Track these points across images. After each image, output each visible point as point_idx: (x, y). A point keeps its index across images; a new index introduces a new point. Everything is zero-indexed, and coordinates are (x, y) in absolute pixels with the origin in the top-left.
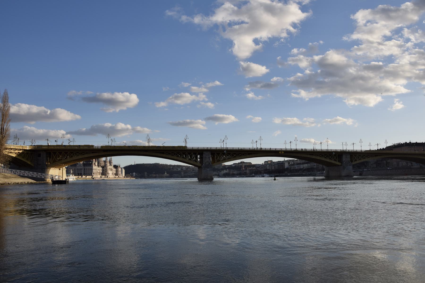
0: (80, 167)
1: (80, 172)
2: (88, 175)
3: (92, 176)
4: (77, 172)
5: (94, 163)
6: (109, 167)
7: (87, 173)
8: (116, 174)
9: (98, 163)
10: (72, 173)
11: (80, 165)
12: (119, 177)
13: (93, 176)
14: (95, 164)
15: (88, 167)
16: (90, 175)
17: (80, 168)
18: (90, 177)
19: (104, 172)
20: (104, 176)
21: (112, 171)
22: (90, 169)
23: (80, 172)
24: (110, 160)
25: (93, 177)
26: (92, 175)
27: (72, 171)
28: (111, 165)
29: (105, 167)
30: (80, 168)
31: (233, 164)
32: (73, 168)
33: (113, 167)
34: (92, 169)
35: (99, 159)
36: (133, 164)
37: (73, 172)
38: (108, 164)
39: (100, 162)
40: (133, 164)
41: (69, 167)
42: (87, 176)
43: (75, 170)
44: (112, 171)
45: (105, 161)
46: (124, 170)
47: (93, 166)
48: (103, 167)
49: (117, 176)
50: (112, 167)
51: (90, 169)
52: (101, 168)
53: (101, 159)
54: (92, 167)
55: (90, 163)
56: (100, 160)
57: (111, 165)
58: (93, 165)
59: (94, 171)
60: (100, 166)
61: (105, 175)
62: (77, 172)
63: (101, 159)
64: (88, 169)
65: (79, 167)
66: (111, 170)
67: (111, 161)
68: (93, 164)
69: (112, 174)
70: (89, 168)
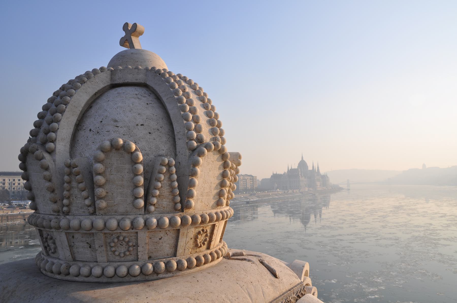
14: (301, 175)
25: (301, 191)
42: (294, 190)
58: (300, 177)
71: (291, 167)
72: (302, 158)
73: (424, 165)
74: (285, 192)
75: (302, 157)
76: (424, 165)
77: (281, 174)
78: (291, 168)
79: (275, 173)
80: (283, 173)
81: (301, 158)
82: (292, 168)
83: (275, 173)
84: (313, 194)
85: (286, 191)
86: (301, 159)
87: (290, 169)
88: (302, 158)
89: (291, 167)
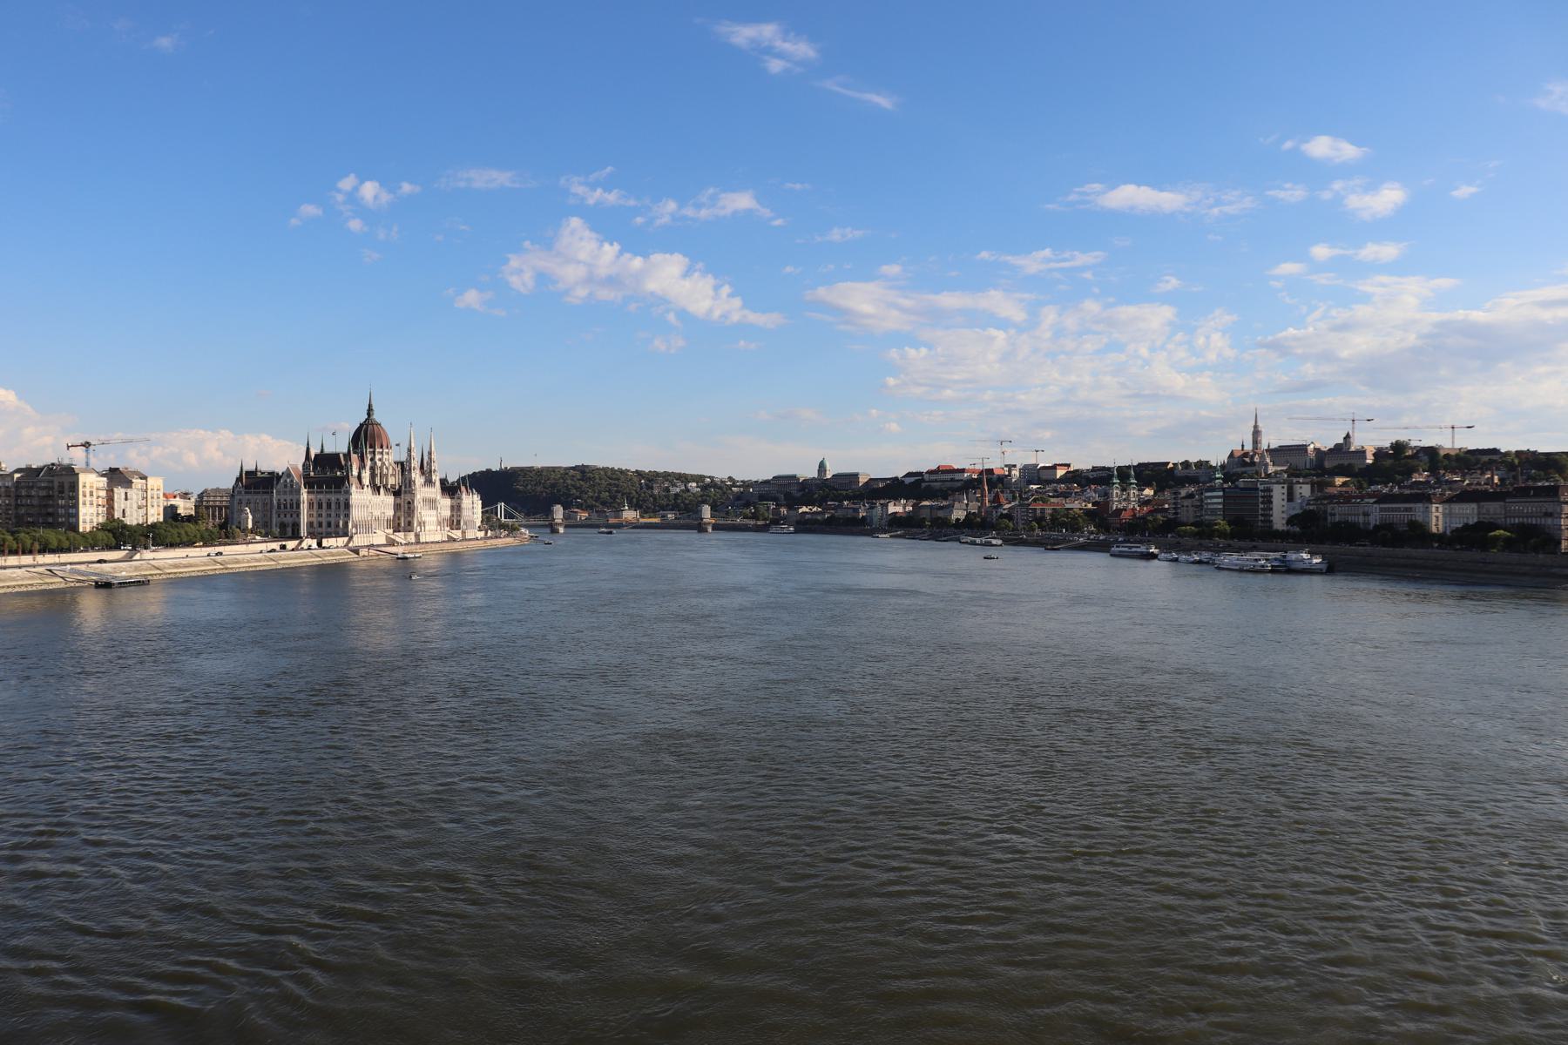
0: (291, 492)
1: (288, 516)
2: (329, 536)
3: (347, 538)
4: (274, 516)
5: (355, 472)
6: (422, 492)
7: (324, 524)
8: (455, 522)
9: (373, 476)
10: (250, 526)
11: (292, 486)
12: (463, 533)
13: (351, 538)
14: (359, 478)
15: (328, 496)
16: (337, 535)
17: (288, 501)
18: (342, 541)
19: (404, 518)
20: (400, 537)
21: (436, 508)
22: (338, 503)
23: (288, 516)
24: (426, 459)
26: (345, 534)
27: (250, 517)
28: (429, 482)
29: (405, 492)
30: (288, 501)
31: (904, 477)
32: (259, 498)
33: (439, 491)
34: (347, 506)
35: (378, 457)
36: (495, 468)
37: (258, 516)
38: (418, 478)
39: (381, 468)
40: (494, 470)
41: (240, 493)
43: (265, 505)
44: (436, 508)
45: (402, 464)
46: (480, 502)
47: (353, 489)
48: (397, 494)
49: (457, 534)
50: (435, 492)
51: (338, 503)
52: (390, 499)
53: (385, 456)
54: (348, 493)
55: (338, 473)
56: (380, 460)
57: (429, 482)
59: (356, 514)
60: (382, 490)
61: (409, 527)
62: (274, 516)
63: (388, 454)
64: (329, 506)
65: (285, 493)
66: (432, 503)
67: (430, 464)
68: (354, 481)
69: (439, 523)
70: (333, 498)
71: (322, 446)
72: (370, 411)
73: (822, 467)
74: (283, 547)
75: (370, 406)
76: (822, 467)
77: (271, 473)
78: (318, 451)
79: (249, 467)
80: (284, 470)
81: (366, 412)
82: (327, 451)
83: (253, 468)
84: (399, 556)
85: (291, 544)
86: (366, 417)
87: (316, 455)
88: (370, 411)
89: (322, 446)
